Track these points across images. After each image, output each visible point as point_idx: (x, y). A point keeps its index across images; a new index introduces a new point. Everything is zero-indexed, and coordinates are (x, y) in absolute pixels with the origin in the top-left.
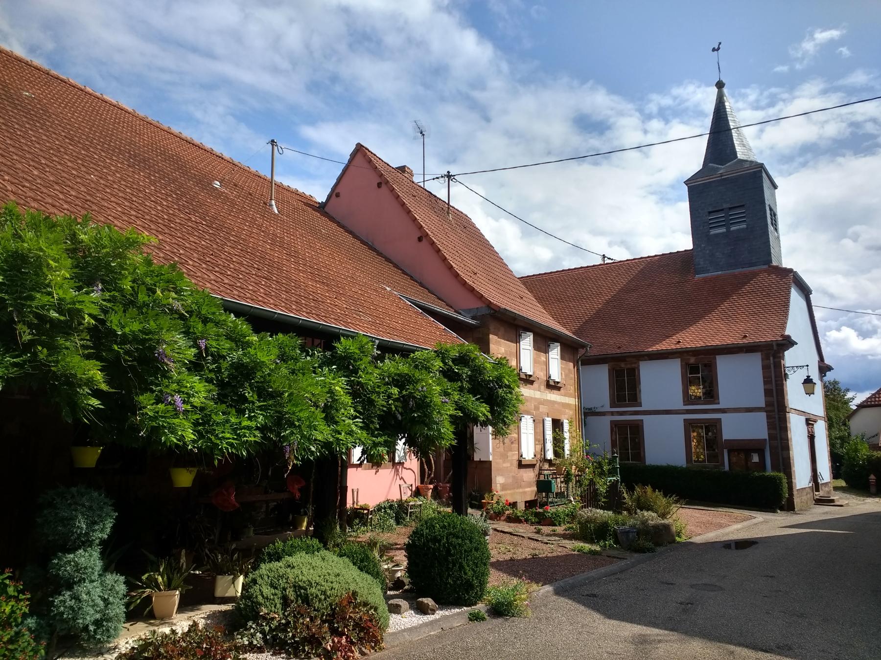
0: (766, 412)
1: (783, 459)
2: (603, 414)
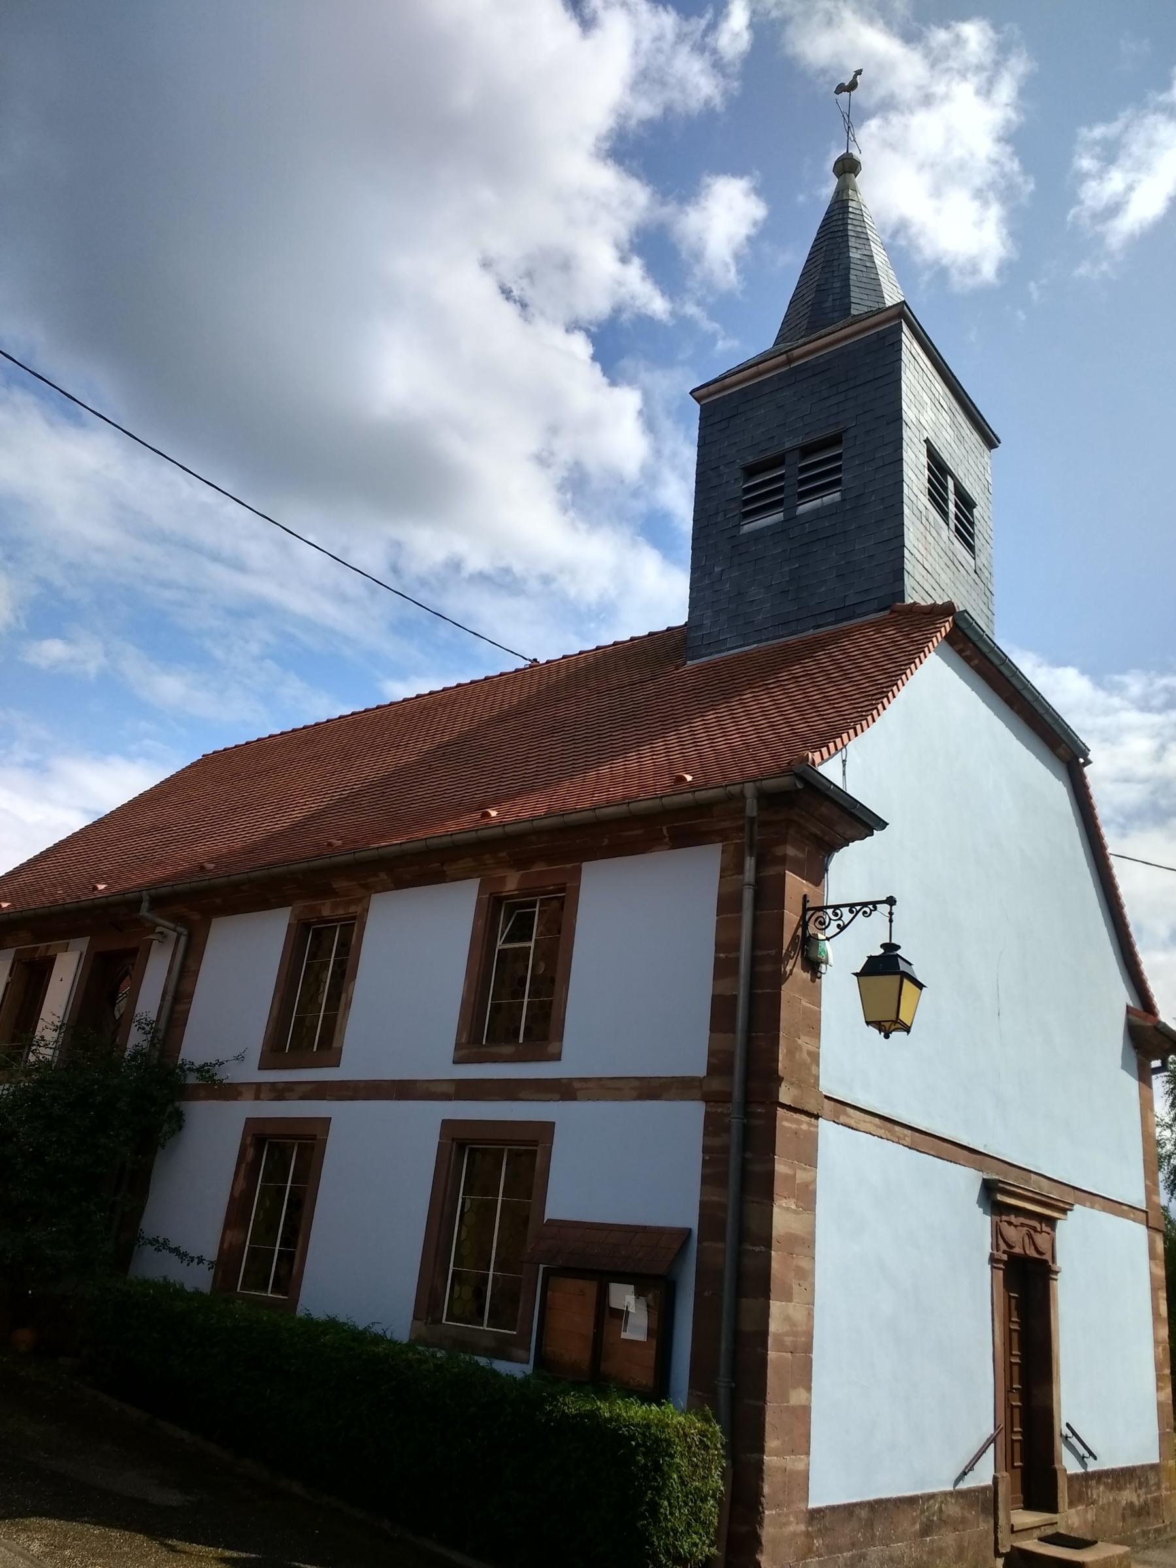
0: (707, 1098)
1: (737, 1335)
2: (230, 1092)
